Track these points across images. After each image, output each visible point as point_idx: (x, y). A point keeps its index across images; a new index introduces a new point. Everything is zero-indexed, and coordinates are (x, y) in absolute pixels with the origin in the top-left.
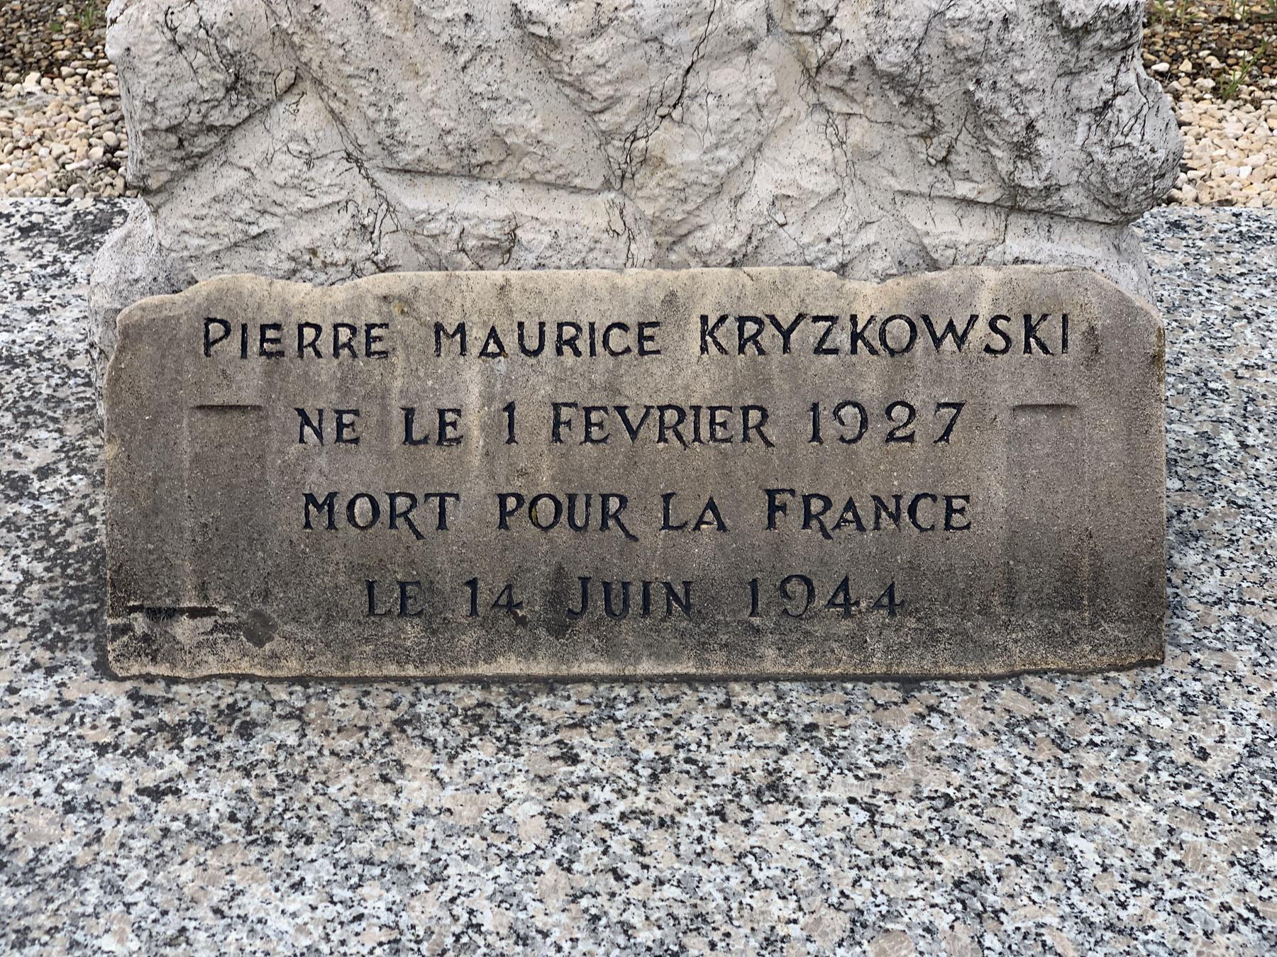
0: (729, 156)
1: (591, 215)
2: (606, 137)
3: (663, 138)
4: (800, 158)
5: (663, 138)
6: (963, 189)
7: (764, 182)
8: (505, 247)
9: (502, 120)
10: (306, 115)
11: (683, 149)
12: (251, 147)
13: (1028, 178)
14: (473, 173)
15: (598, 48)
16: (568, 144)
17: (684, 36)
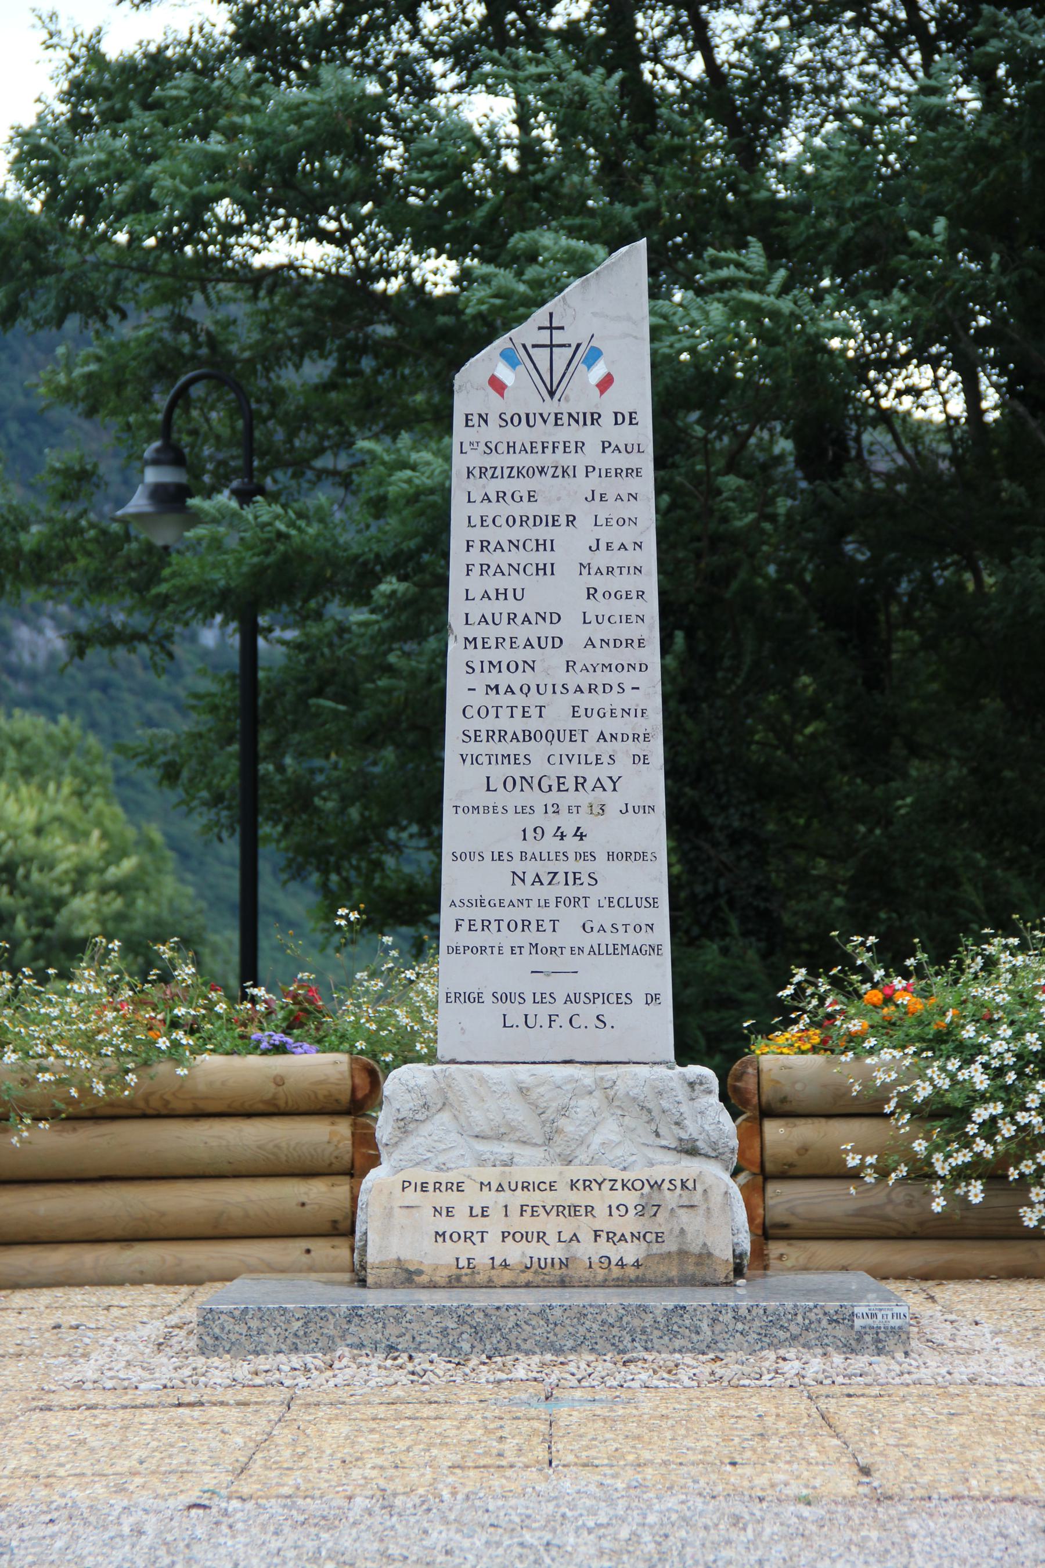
0: (586, 1130)
1: (539, 1153)
2: (544, 1123)
3: (562, 1122)
4: (610, 1130)
5: (562, 1122)
6: (664, 1143)
7: (596, 1140)
8: (509, 1163)
9: (510, 1116)
10: (445, 1117)
11: (568, 1126)
12: (426, 1129)
13: (685, 1136)
14: (500, 1137)
15: (541, 1090)
16: (532, 1128)
17: (568, 1087)
